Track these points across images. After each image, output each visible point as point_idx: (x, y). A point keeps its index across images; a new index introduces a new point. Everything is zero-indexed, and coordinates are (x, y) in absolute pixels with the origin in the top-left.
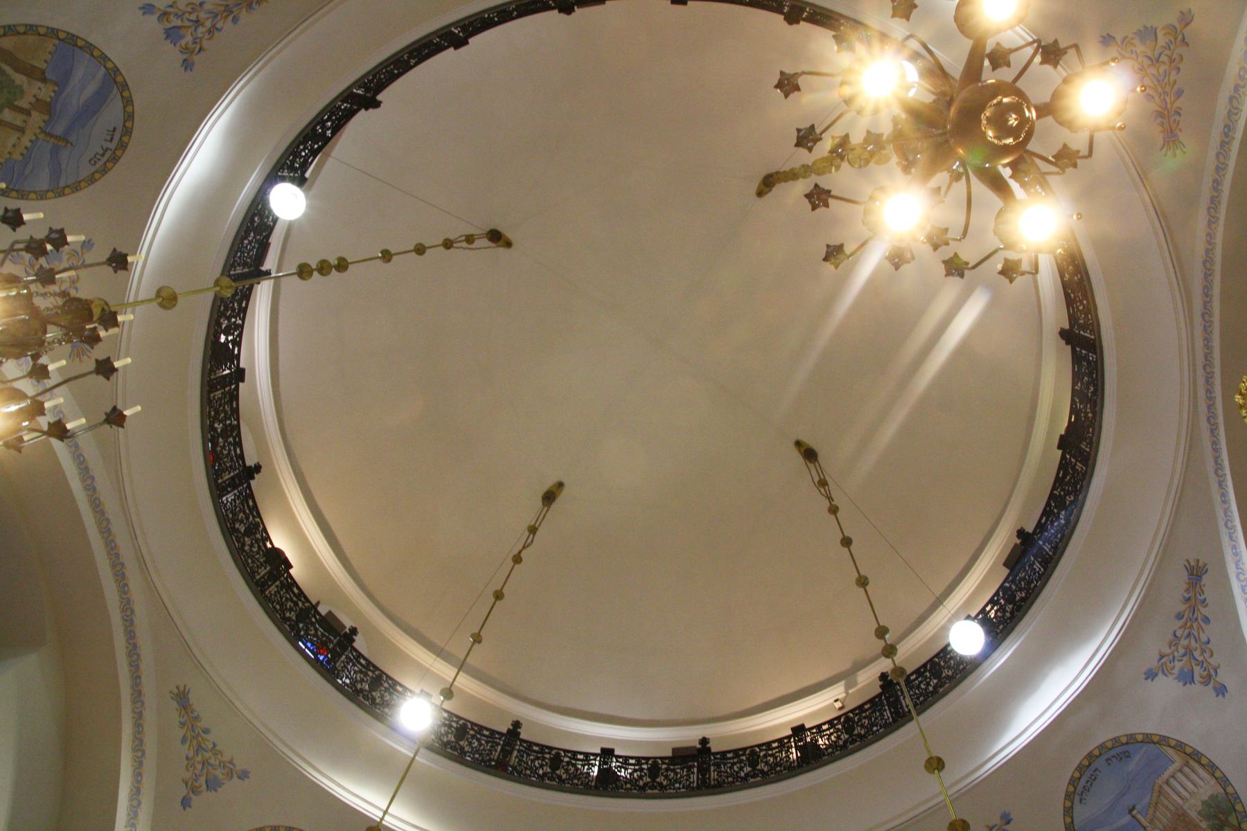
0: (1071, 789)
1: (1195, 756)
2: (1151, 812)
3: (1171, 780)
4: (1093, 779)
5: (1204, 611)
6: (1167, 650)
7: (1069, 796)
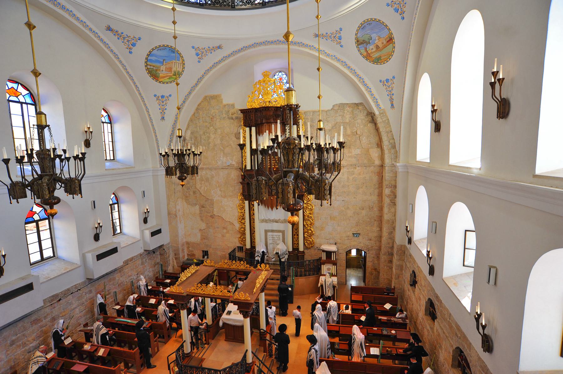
1: (184, 64)
7: (156, 47)
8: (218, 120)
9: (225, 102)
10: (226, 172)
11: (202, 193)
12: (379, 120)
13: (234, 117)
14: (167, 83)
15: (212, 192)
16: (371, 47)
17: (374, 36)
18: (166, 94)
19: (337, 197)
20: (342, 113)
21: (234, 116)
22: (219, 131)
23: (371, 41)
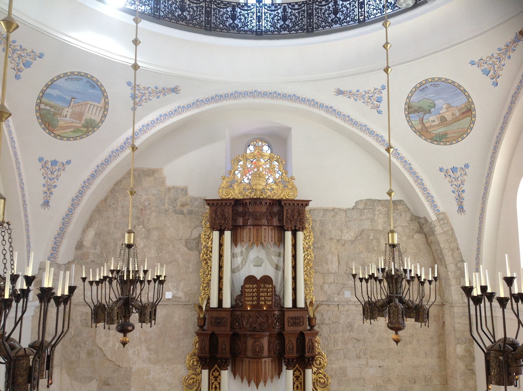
0: (69, 74)
1: (106, 110)
2: (78, 104)
3: (92, 106)
4: (78, 80)
5: (161, 95)
6: (141, 87)
7: (65, 74)
8: (154, 214)
9: (169, 183)
11: (108, 355)
12: (438, 230)
13: (185, 210)
14: (68, 139)
16: (431, 118)
17: (439, 103)
18: (62, 159)
19: (371, 362)
20: (370, 215)
21: (185, 210)
22: (155, 233)
23: (432, 110)
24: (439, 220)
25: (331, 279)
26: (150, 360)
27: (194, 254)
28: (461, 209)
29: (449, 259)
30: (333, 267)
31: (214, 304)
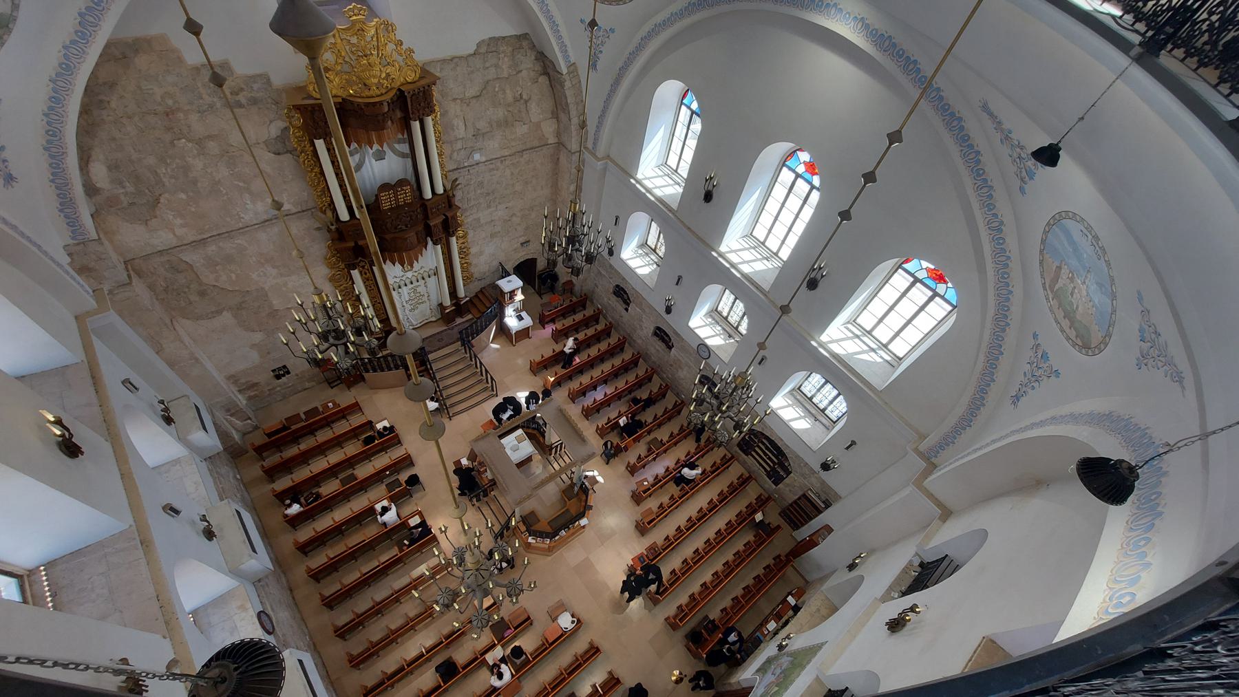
10: (276, 229)
12: (568, 84)
13: (242, 98)
15: (254, 276)
22: (213, 147)
24: (569, 73)
25: (459, 145)
26: (282, 275)
27: (287, 159)
28: (593, 65)
29: (573, 113)
30: (461, 132)
31: (344, 216)
